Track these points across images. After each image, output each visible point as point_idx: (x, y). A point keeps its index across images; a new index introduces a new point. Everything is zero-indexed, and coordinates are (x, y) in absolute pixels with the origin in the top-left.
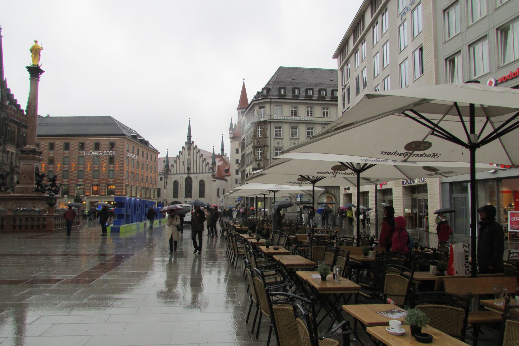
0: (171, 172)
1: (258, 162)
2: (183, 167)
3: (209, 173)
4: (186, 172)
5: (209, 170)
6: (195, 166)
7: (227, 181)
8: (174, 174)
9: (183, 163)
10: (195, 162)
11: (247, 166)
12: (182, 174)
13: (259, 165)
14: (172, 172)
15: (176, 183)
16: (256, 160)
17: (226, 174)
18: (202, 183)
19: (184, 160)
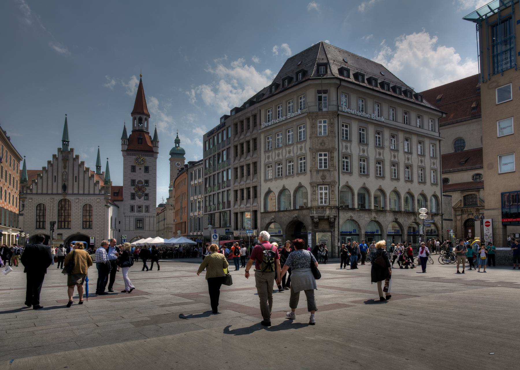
0: (31, 190)
1: (321, 174)
2: (55, 184)
3: (99, 194)
4: (60, 191)
5: (100, 191)
6: (76, 184)
7: (118, 207)
8: (37, 194)
9: (55, 179)
10: (76, 179)
11: (266, 180)
12: (52, 194)
13: (324, 177)
14: (34, 191)
15: (41, 209)
16: (318, 171)
17: (116, 198)
18: (87, 210)
19: (55, 174)
